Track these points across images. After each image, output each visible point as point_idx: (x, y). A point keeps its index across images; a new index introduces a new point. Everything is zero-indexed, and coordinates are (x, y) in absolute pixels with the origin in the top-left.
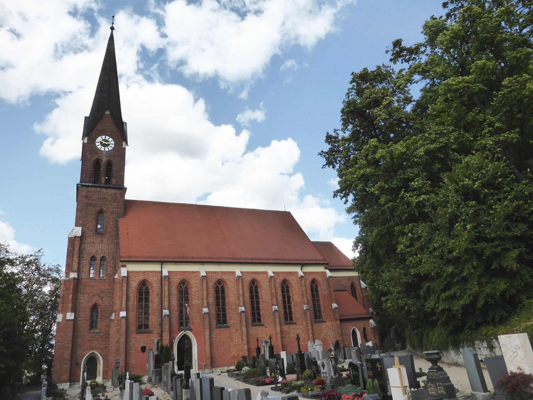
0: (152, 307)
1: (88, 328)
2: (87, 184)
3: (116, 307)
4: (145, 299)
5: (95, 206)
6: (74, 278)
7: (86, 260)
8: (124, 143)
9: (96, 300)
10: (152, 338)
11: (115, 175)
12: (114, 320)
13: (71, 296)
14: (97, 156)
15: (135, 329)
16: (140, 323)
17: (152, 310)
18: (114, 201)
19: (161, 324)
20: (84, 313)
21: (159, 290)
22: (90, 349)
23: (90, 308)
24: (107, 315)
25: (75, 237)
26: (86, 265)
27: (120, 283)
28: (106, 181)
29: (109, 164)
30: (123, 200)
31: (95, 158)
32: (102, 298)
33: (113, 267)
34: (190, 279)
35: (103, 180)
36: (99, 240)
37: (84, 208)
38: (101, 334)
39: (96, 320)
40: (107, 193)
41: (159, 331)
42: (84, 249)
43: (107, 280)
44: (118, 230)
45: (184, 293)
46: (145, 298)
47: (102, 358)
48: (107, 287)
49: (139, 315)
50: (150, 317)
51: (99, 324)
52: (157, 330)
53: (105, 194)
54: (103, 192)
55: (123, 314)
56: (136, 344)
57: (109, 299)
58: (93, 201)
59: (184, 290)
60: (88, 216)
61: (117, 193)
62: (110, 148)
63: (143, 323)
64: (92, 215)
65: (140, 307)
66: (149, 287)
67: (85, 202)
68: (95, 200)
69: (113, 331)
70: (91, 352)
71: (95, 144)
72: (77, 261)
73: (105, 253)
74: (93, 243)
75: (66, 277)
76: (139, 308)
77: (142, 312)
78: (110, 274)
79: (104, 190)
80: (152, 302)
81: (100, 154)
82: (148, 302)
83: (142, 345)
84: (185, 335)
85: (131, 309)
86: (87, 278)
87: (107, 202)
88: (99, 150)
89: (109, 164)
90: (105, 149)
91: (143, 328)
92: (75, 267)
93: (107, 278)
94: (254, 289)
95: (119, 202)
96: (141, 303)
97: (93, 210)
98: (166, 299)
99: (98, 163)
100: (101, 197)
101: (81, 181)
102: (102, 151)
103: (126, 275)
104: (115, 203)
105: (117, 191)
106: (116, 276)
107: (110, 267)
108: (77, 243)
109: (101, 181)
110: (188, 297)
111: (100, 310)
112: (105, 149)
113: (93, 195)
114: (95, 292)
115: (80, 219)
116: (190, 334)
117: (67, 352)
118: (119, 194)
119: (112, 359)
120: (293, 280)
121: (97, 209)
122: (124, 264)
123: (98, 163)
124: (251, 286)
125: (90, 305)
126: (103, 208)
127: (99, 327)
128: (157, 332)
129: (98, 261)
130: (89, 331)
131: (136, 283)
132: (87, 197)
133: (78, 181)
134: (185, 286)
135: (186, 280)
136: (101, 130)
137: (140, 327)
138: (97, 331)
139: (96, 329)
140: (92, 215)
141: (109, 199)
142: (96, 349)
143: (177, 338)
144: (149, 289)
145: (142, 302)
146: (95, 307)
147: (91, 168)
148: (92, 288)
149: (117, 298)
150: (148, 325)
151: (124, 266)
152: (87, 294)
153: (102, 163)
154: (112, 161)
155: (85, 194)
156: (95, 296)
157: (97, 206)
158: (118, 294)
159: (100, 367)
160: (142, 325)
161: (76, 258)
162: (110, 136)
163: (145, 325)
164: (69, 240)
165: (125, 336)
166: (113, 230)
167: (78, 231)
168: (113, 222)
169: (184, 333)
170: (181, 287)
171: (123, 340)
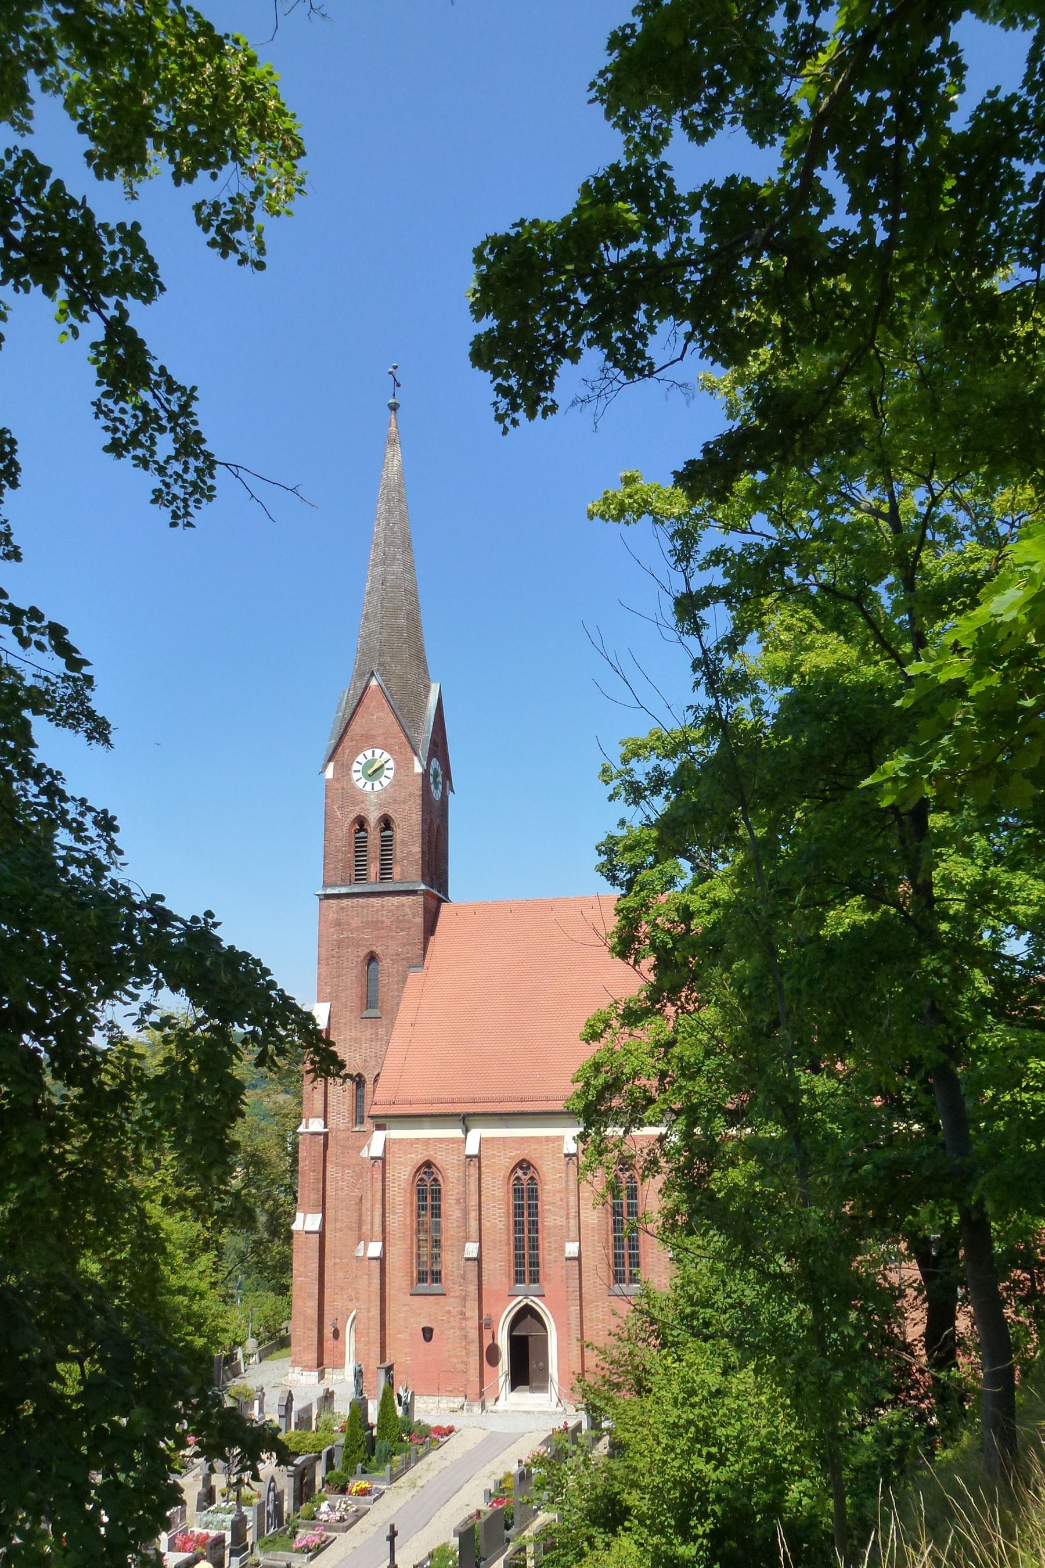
5: (358, 946)
14: (357, 808)
31: (353, 816)
34: (541, 1157)
35: (374, 869)
36: (368, 1033)
40: (383, 906)
45: (525, 1195)
66: (440, 1178)
68: (357, 929)
71: (351, 779)
74: (357, 1040)
84: (527, 1305)
86: (348, 1129)
87: (383, 932)
89: (386, 823)
98: (474, 1214)
99: (361, 823)
101: (326, 885)
102: (366, 794)
103: (379, 1154)
105: (403, 899)
116: (540, 1306)
121: (364, 952)
122: (380, 1121)
123: (361, 823)
126: (374, 948)
128: (458, 1294)
132: (338, 924)
137: (422, 1278)
151: (380, 1127)
152: (349, 1167)
163: (432, 1272)
168: (398, 982)
169: (525, 1301)
170: (518, 1178)
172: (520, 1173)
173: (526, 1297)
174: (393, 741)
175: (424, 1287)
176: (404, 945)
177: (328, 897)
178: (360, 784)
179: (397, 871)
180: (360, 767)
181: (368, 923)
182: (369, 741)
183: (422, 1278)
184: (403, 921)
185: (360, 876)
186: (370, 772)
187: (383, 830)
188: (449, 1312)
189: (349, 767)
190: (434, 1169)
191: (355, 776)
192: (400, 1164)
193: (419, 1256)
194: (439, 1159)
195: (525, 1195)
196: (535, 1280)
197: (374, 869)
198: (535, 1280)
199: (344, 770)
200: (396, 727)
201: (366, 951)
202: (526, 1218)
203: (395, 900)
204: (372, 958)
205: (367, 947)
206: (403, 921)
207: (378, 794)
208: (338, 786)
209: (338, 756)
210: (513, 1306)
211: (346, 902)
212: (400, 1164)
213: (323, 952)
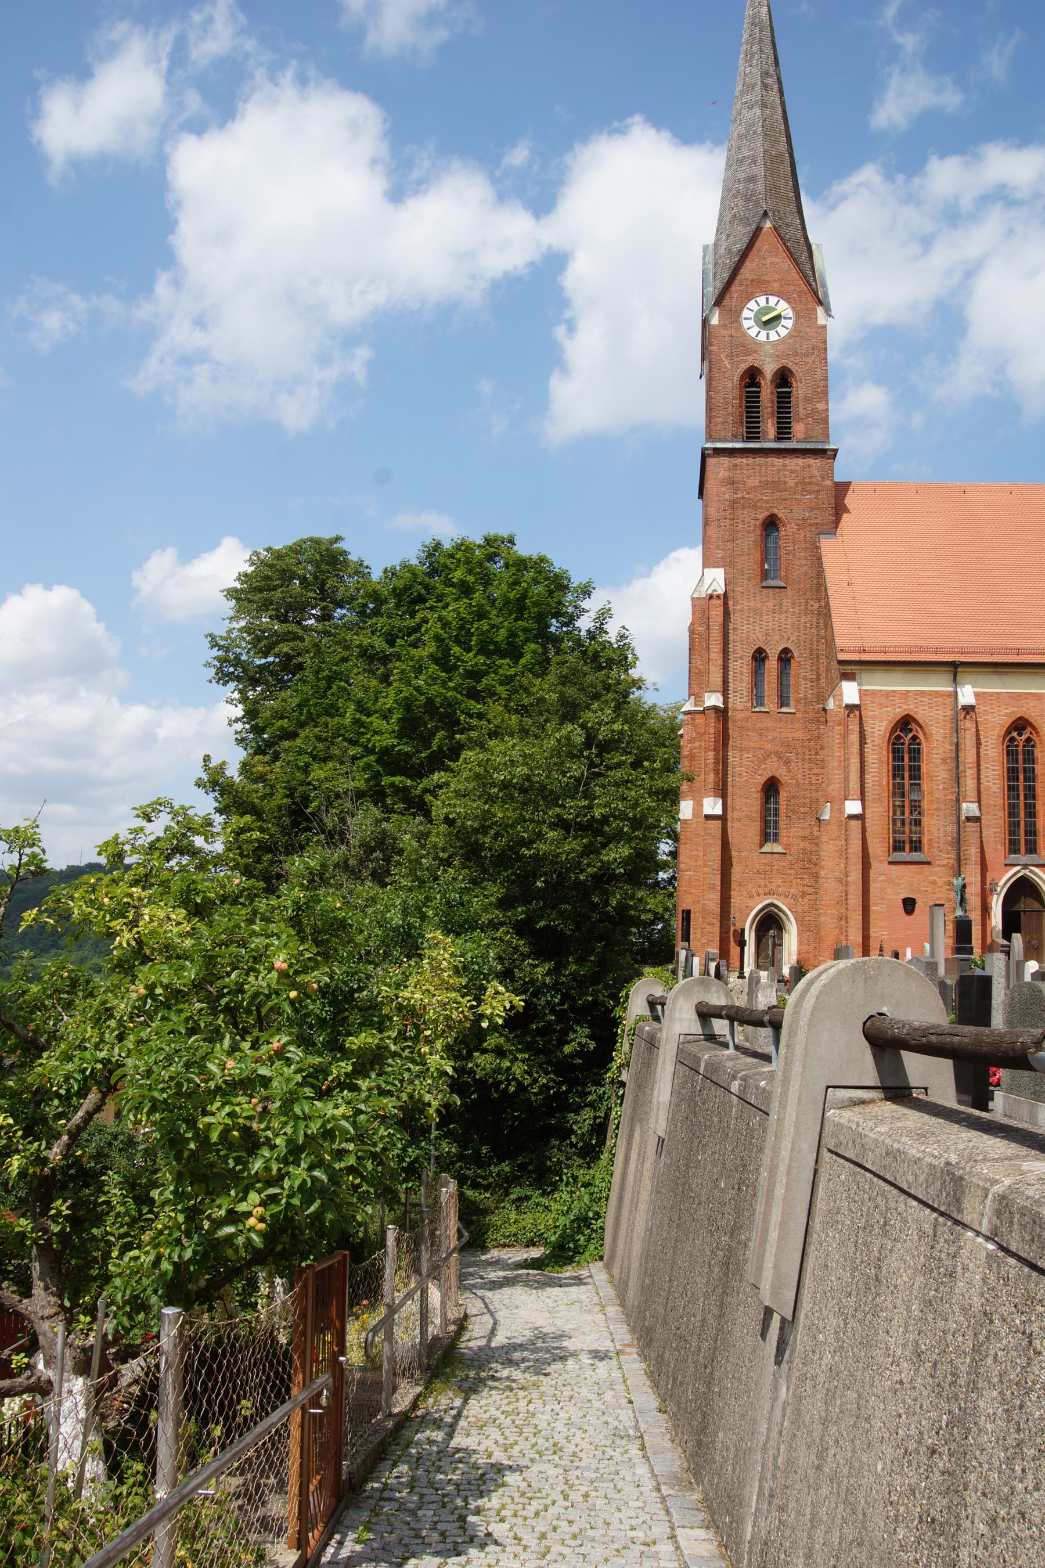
0: (931, 793)
1: (757, 840)
2: (729, 445)
3: (834, 788)
4: (910, 770)
5: (755, 507)
6: (715, 708)
7: (741, 658)
8: (820, 310)
9: (773, 768)
10: (932, 878)
11: (802, 412)
12: (828, 823)
13: (711, 754)
14: (750, 359)
15: (886, 849)
16: (898, 836)
17: (931, 802)
18: (803, 490)
19: (958, 842)
20: (743, 800)
21: (948, 747)
22: (765, 894)
23: (759, 789)
24: (802, 809)
25: (711, 597)
26: (742, 674)
27: (839, 724)
28: (778, 433)
29: (783, 378)
30: (828, 483)
31: (744, 367)
32: (787, 763)
36: (770, 604)
37: (727, 514)
38: (790, 858)
39: (776, 822)
40: (785, 466)
41: (951, 861)
43: (799, 715)
44: (820, 573)
45: (1020, 757)
46: (910, 766)
47: (796, 919)
48: (799, 735)
49: (895, 813)
50: (925, 821)
51: (783, 833)
52: (947, 858)
54: (773, 466)
55: (853, 807)
56: (889, 891)
57: (807, 766)
58: (748, 493)
59: (1020, 748)
60: (739, 535)
61: (809, 466)
62: (783, 332)
63: (905, 837)
65: (898, 791)
66: (921, 736)
67: (727, 496)
69: (829, 849)
71: (740, 326)
72: (720, 662)
73: (788, 639)
75: (696, 705)
76: (894, 794)
77: (903, 806)
79: (777, 462)
80: (931, 778)
81: (755, 352)
82: (919, 779)
83: (903, 896)
85: (870, 796)
86: (747, 709)
88: (754, 341)
89: (783, 378)
90: (768, 338)
91: (907, 848)
92: (716, 676)
93: (798, 710)
95: (819, 491)
96: (898, 780)
97: (752, 520)
98: (970, 773)
99: (752, 376)
100: (770, 479)
102: (760, 344)
103: (857, 702)
105: (810, 461)
107: (805, 678)
108: (716, 613)
109: (766, 433)
110: (1033, 768)
111: (783, 795)
112: (768, 338)
113: (748, 477)
114: (769, 747)
115: (717, 547)
117: (711, 896)
119: (828, 921)
121: (762, 515)
122: (849, 669)
123: (752, 376)
125: (761, 780)
126: (775, 511)
127: (783, 839)
128: (945, 862)
129: (772, 664)
130: (761, 847)
131: (884, 724)
132: (731, 482)
134: (1023, 738)
135: (1027, 720)
136: (753, 281)
137: (898, 847)
138: (778, 848)
139: (775, 845)
141: (791, 483)
142: (778, 895)
143: (1001, 883)
144: (919, 744)
145: (903, 779)
146: (771, 788)
147: (734, 398)
148: (760, 734)
149: (836, 764)
150: (920, 842)
152: (748, 750)
153: (764, 379)
154: (790, 371)
155: (727, 474)
156: (768, 756)
157: (761, 508)
158: (837, 754)
159: (789, 941)
160: (904, 842)
161: (716, 654)
162: (781, 295)
164: (694, 606)
165: (860, 866)
167: (716, 579)
170: (1012, 739)
171: (855, 875)
172: (1015, 734)
173: (1025, 866)
174: (791, 288)
175: (904, 856)
177: (718, 452)
178: (752, 333)
179: (798, 429)
180: (751, 315)
181: (767, 483)
182: (761, 287)
183: (898, 847)
184: (810, 483)
185: (753, 434)
186: (765, 319)
187: (778, 387)
188: (934, 882)
189: (739, 313)
190: (914, 726)
191: (746, 324)
192: (873, 718)
193: (894, 820)
194: (921, 714)
195: (1020, 757)
196: (1032, 849)
197: (770, 427)
198: (1032, 849)
199: (734, 317)
200: (794, 274)
201: (767, 514)
202: (1021, 783)
204: (771, 524)
206: (810, 483)
207: (774, 344)
208: (723, 332)
209: (726, 301)
210: (1005, 879)
212: (873, 718)
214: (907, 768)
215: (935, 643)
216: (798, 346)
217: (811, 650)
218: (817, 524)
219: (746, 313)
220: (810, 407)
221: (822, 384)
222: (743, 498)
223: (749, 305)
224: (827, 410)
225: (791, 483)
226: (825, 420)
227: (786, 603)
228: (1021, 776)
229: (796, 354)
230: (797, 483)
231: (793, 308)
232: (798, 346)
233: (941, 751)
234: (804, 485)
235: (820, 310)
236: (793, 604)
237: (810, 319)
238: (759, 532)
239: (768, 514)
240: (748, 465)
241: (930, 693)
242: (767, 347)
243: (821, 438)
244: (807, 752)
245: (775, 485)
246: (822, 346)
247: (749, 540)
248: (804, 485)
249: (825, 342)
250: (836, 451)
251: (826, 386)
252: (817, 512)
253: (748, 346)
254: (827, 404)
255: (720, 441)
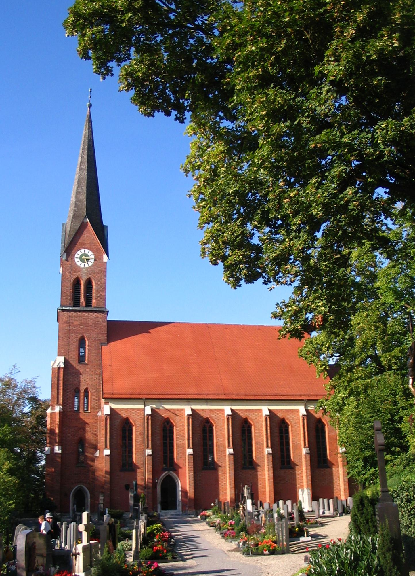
2: (68, 308)
5: (77, 333)
14: (77, 274)
18: (95, 326)
31: (75, 277)
33: (96, 400)
37: (66, 335)
40: (89, 317)
42: (68, 380)
53: (86, 319)
58: (74, 327)
61: (98, 317)
64: (74, 342)
67: (66, 328)
70: (79, 485)
73: (88, 384)
78: (94, 407)
81: (79, 271)
94: (246, 429)
95: (101, 327)
97: (75, 338)
100: (83, 322)
101: (62, 306)
103: (109, 413)
104: (97, 328)
105: (98, 314)
106: (99, 414)
118: (101, 318)
120: (293, 419)
121: (79, 336)
122: (107, 400)
124: (243, 426)
126: (84, 334)
131: (119, 421)
132: (68, 323)
133: (58, 305)
140: (74, 342)
141: (91, 324)
145: (126, 441)
151: (106, 403)
156: (80, 429)
166: (95, 359)
176: (98, 334)
177: (63, 310)
180: (78, 256)
181: (82, 323)
184: (98, 324)
191: (76, 260)
201: (81, 335)
203: (95, 315)
205: (81, 334)
206: (98, 324)
207: (87, 269)
211: (72, 314)
213: (60, 335)
214: (127, 437)
215: (138, 391)
216: (95, 270)
217: (97, 389)
218: (100, 340)
219: (76, 256)
220: (99, 294)
221: (104, 285)
222: (72, 329)
223: (78, 253)
224: (105, 295)
225: (91, 324)
226: (105, 299)
227: (88, 370)
228: (168, 439)
229: (94, 273)
230: (93, 324)
231: (94, 255)
232: (95, 270)
233: (139, 430)
234: (96, 325)
235: (105, 256)
236: (90, 370)
237: (101, 259)
238: (78, 342)
239: (81, 335)
240: (74, 316)
241: (135, 409)
242: (84, 269)
243: (103, 306)
244: (94, 428)
245: (85, 324)
246: (105, 270)
247: (74, 345)
248: (96, 325)
249: (106, 269)
250: (108, 312)
251: (106, 286)
252: (100, 335)
253: (77, 269)
254: (106, 293)
255: (65, 306)
